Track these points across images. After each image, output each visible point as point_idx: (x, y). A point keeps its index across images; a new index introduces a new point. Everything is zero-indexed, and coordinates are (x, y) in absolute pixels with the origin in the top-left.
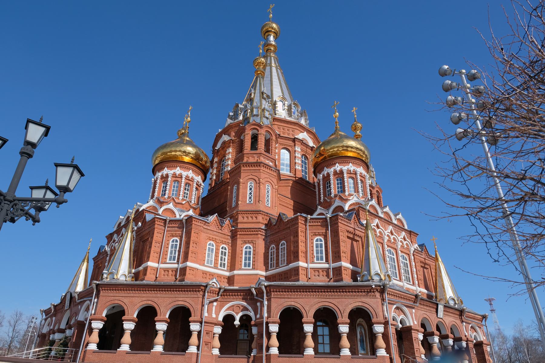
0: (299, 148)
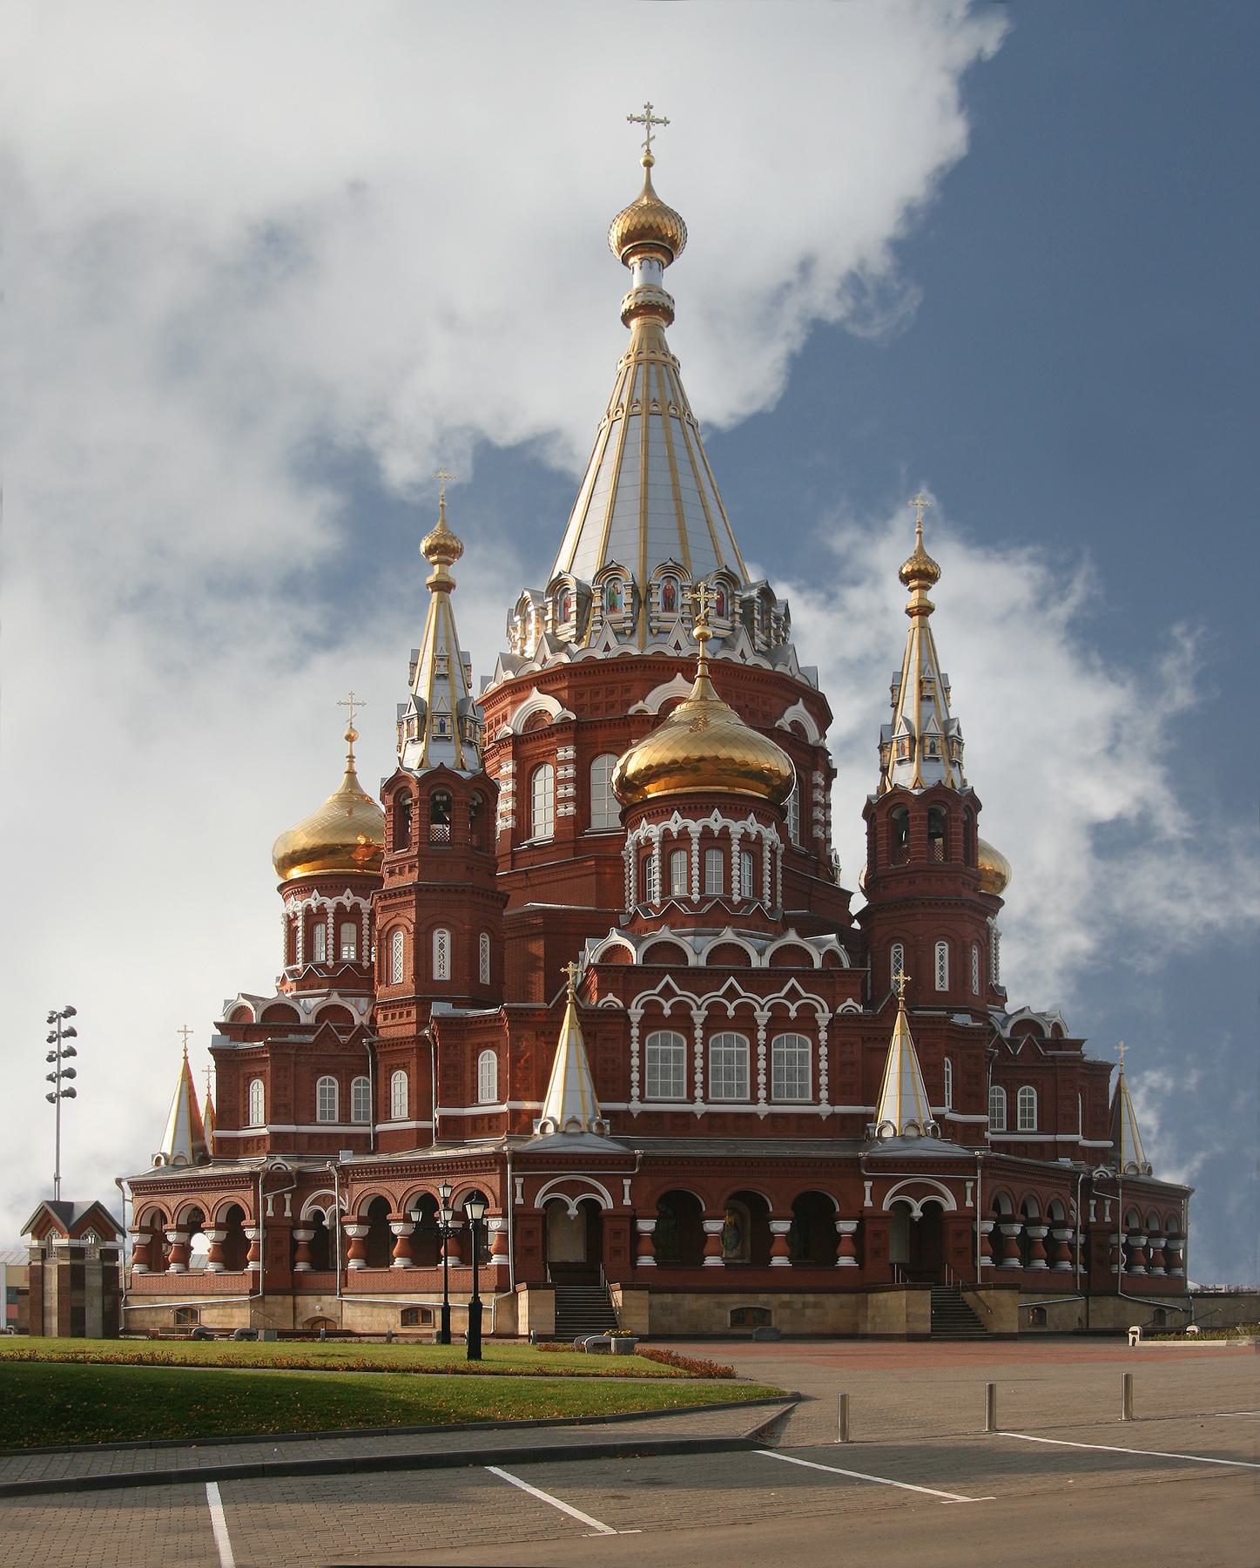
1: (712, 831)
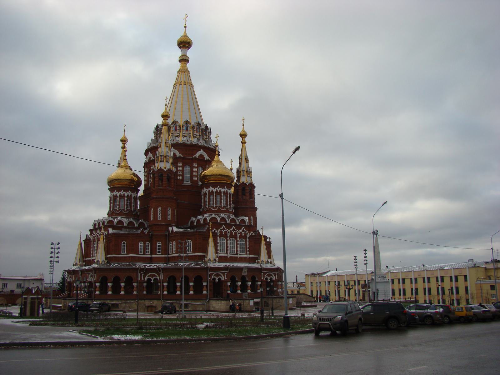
0: (196, 164)
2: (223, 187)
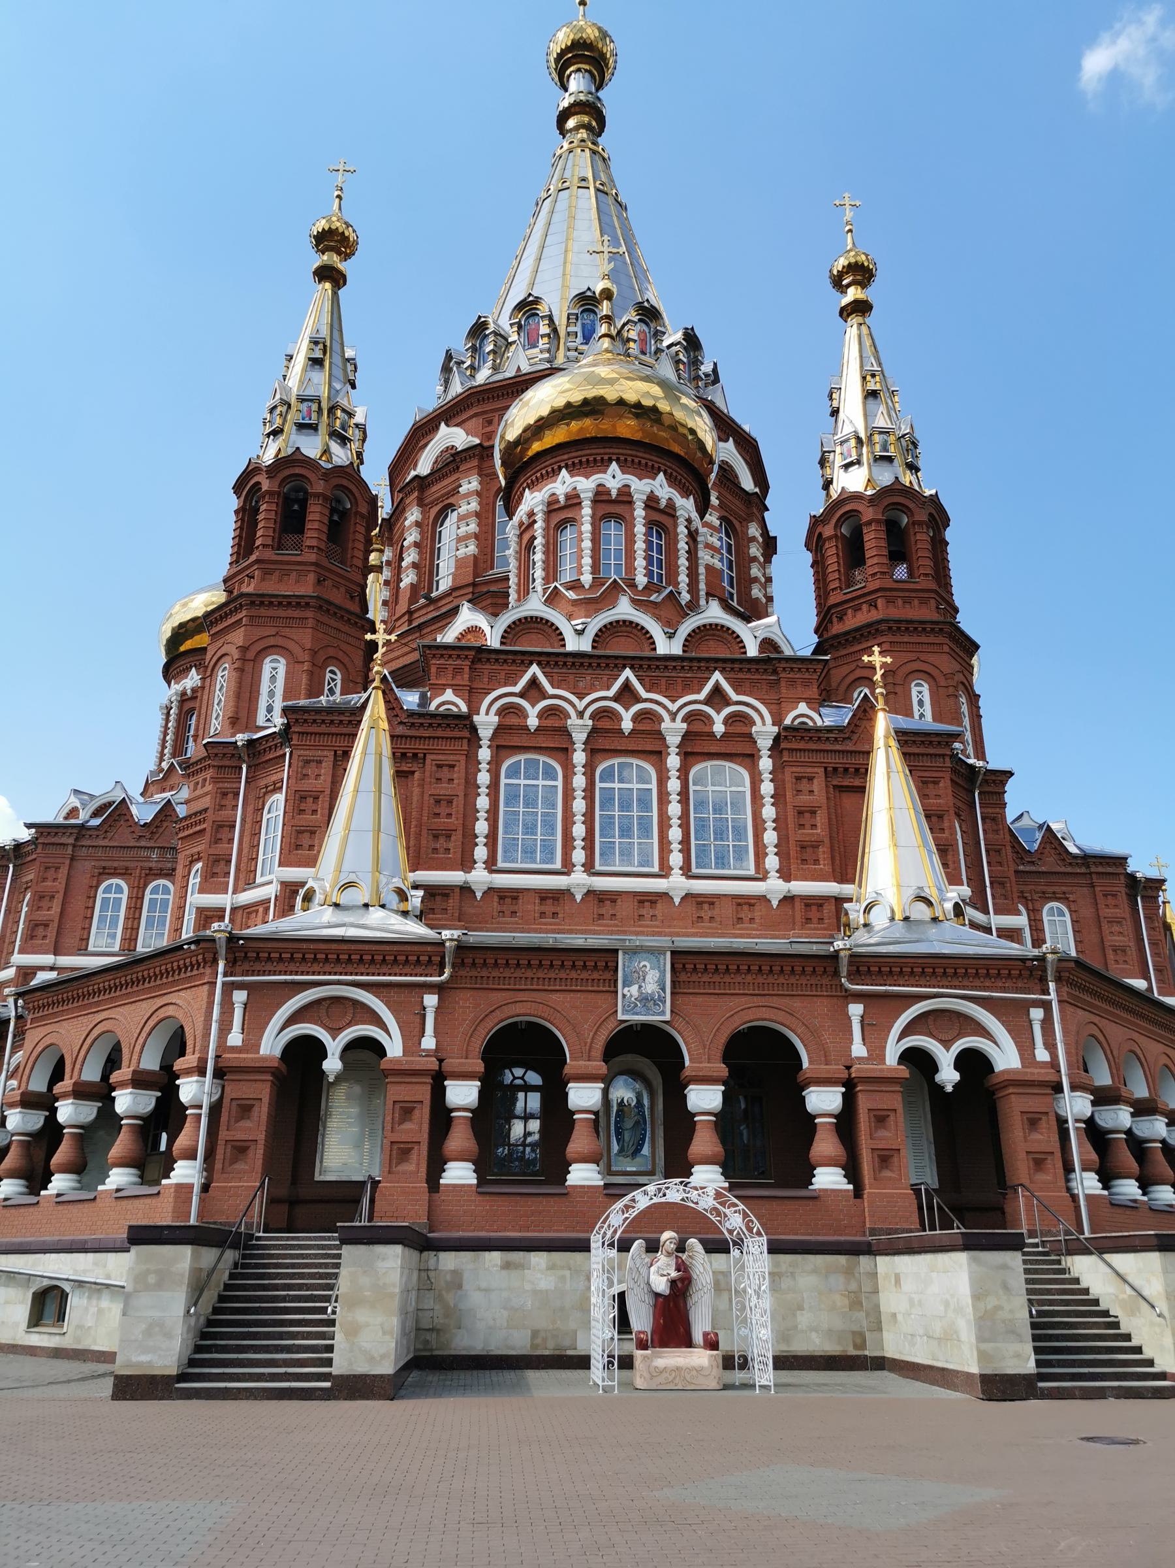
1: (608, 493)
2: (647, 471)
